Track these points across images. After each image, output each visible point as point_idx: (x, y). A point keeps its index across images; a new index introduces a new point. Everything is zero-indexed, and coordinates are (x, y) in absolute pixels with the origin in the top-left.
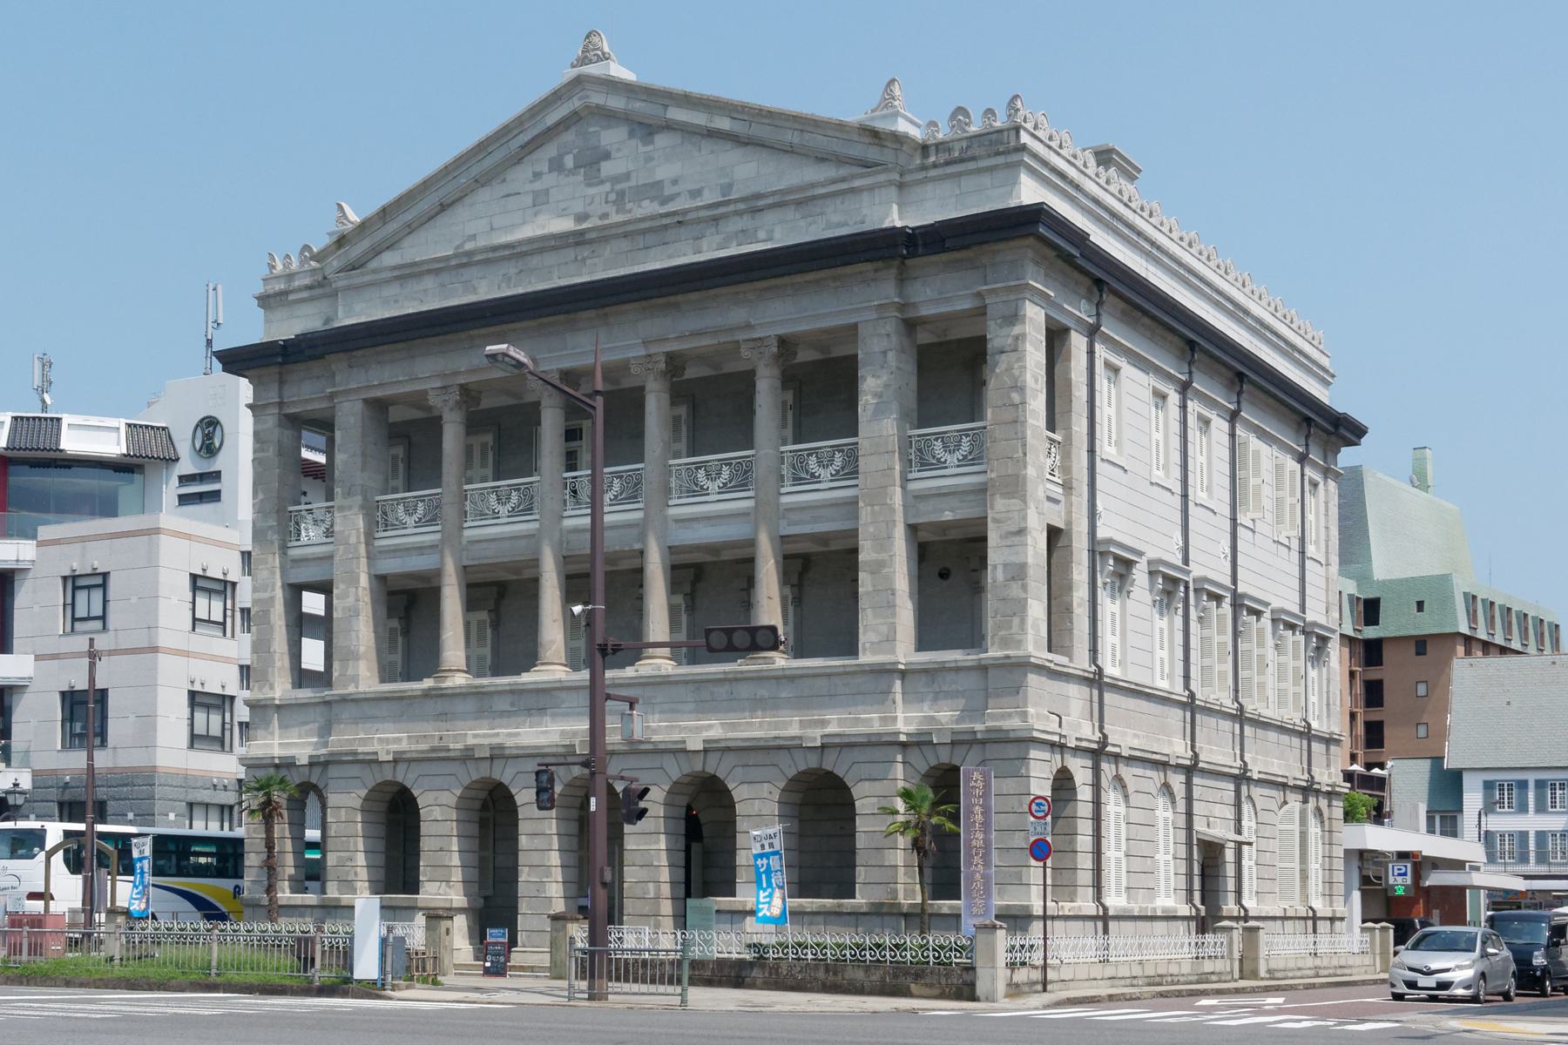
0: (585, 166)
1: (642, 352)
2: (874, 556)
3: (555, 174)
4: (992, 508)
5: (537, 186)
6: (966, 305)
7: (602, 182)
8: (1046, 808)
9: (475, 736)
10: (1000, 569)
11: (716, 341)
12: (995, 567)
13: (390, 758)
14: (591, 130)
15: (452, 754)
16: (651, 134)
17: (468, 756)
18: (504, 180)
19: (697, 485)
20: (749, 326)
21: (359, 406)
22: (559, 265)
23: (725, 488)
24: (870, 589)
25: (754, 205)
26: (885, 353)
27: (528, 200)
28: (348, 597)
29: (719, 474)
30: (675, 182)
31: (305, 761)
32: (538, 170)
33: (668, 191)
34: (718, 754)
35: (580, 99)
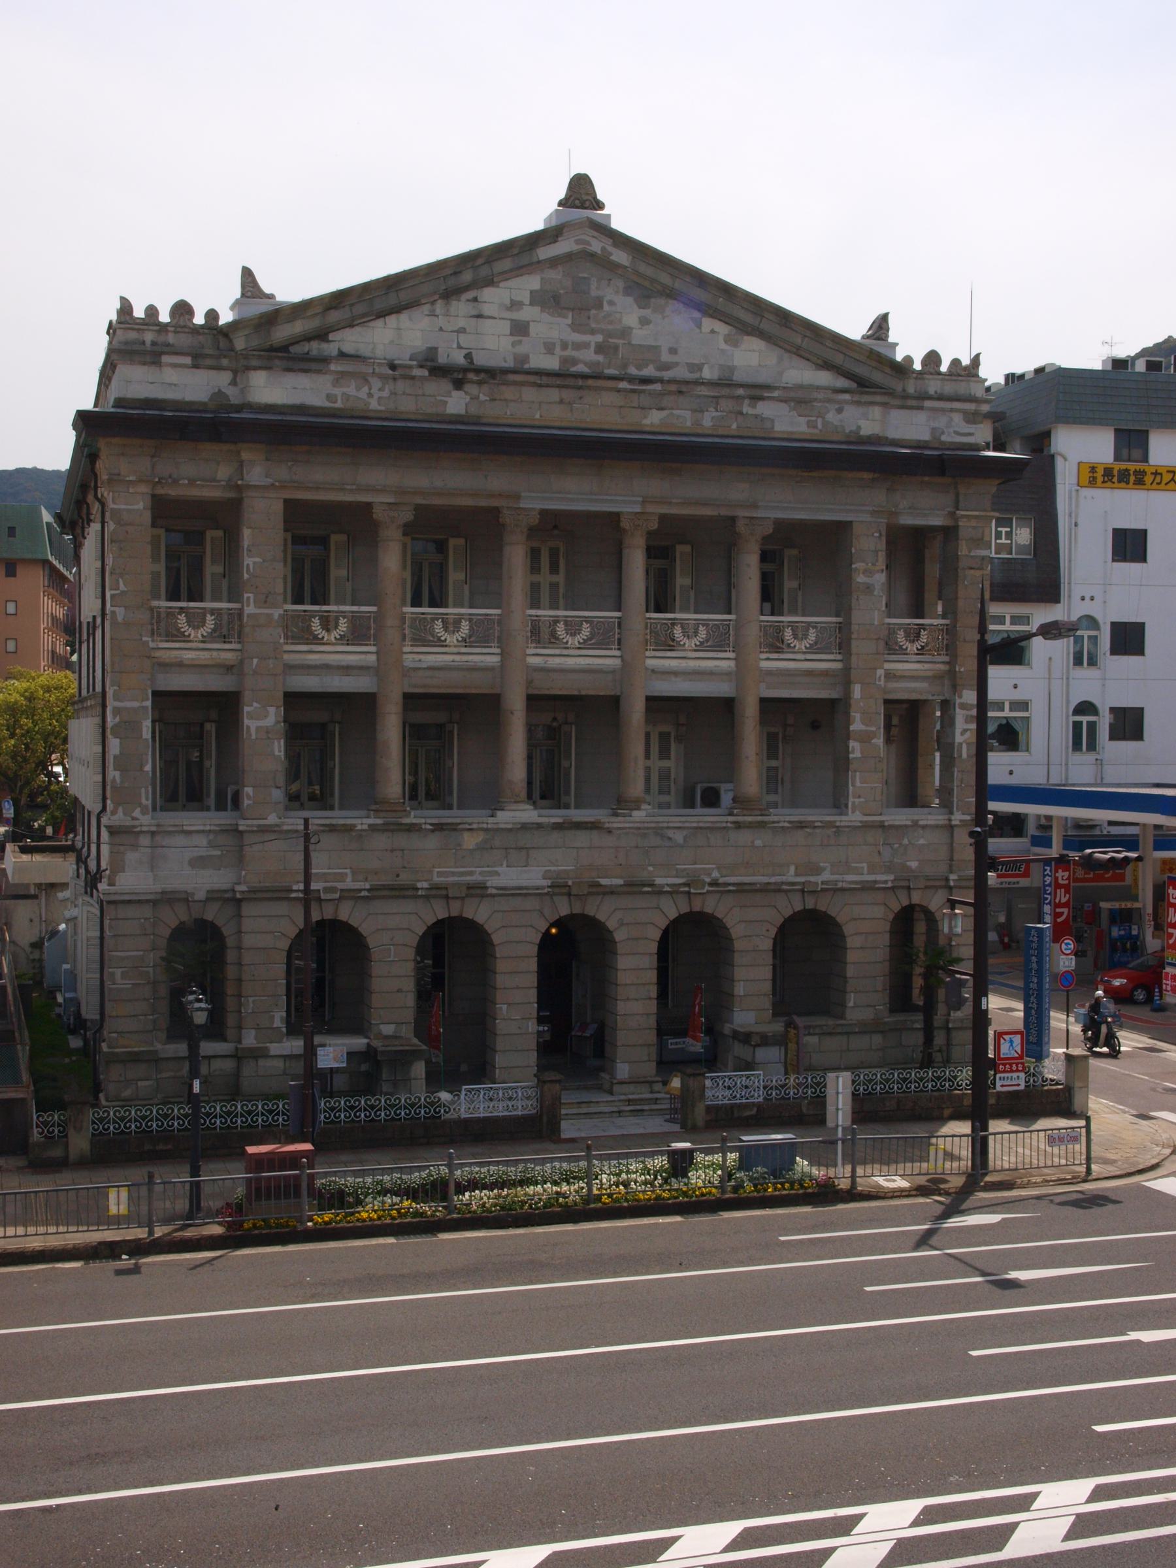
0: (573, 310)
1: (638, 509)
2: (863, 727)
3: (537, 309)
4: (960, 697)
5: (516, 315)
6: (937, 521)
7: (593, 332)
8: (1072, 946)
9: (440, 874)
10: (964, 747)
11: (715, 513)
12: (961, 744)
13: (337, 896)
14: (581, 275)
15: (420, 893)
16: (649, 297)
17: (439, 892)
18: (475, 300)
19: (673, 640)
20: (754, 506)
21: (278, 507)
22: (540, 403)
23: (700, 647)
24: (859, 755)
25: (758, 391)
26: (876, 552)
27: (506, 327)
28: (266, 717)
29: (696, 633)
30: (673, 351)
31: (201, 895)
32: (518, 298)
33: (665, 357)
34: (718, 895)
35: (577, 242)
